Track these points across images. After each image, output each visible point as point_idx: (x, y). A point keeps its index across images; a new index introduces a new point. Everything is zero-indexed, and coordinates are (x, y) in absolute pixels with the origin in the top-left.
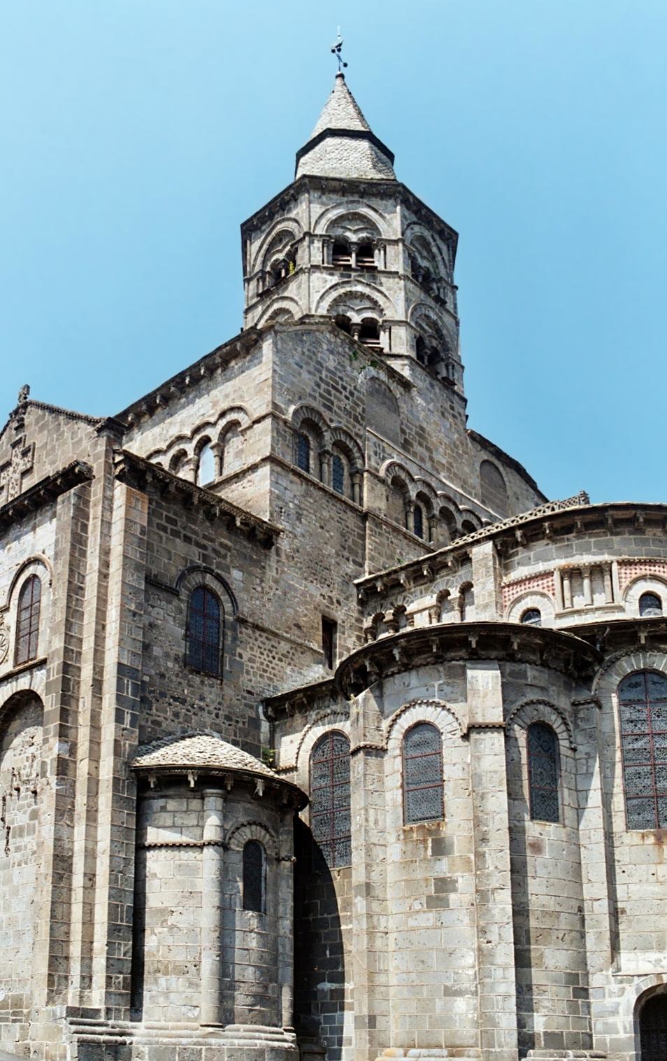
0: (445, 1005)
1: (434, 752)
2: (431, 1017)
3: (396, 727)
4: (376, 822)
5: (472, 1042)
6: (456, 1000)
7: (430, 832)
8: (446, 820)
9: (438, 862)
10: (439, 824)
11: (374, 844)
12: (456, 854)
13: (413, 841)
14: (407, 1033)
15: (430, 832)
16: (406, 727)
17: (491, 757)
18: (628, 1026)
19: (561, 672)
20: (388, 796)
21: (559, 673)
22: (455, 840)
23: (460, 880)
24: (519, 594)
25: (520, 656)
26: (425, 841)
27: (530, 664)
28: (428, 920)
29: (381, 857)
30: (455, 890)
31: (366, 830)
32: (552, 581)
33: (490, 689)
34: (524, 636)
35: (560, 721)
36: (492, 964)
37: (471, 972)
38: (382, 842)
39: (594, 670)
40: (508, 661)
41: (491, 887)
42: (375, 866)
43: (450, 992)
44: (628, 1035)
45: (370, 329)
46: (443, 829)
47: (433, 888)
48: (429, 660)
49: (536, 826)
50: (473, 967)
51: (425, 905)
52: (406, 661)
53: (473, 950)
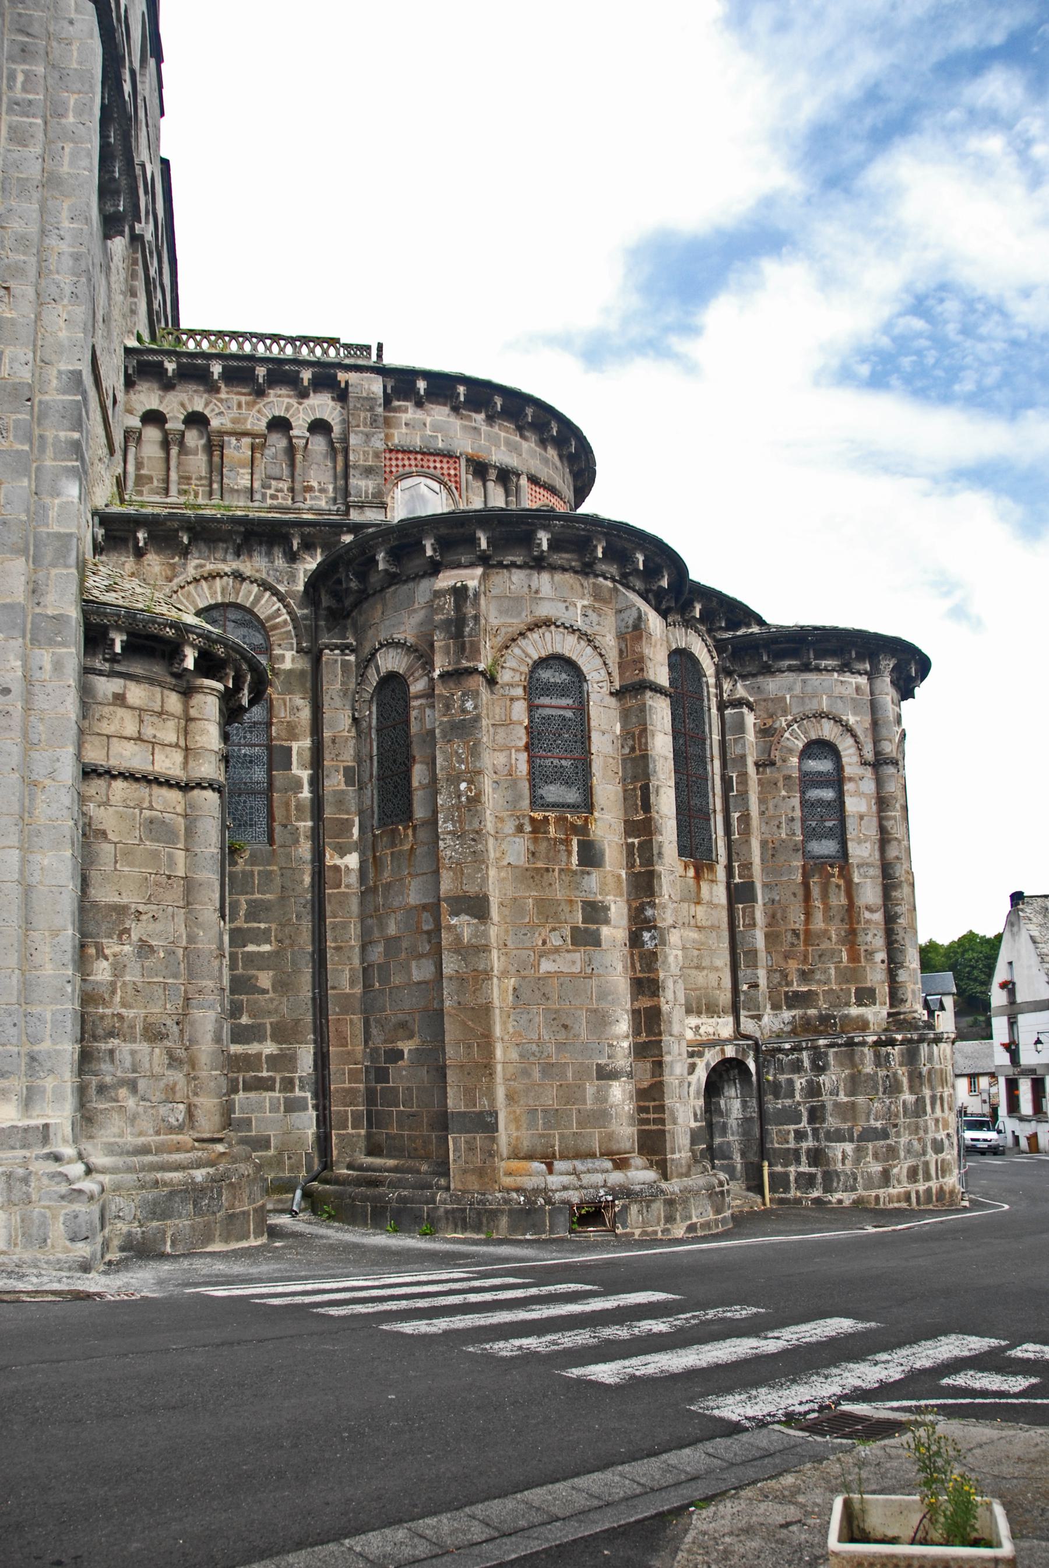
0: (598, 1092)
2: (579, 1111)
7: (575, 829)
8: (596, 814)
9: (586, 877)
10: (586, 818)
12: (608, 868)
13: (548, 839)
14: (542, 1136)
15: (575, 829)
16: (536, 657)
18: (699, 1112)
22: (606, 846)
24: (407, 469)
26: (567, 842)
28: (574, 963)
30: (607, 922)
32: (455, 469)
37: (625, 1044)
43: (606, 1074)
44: (698, 1124)
46: (592, 827)
50: (627, 1037)
53: (627, 1011)
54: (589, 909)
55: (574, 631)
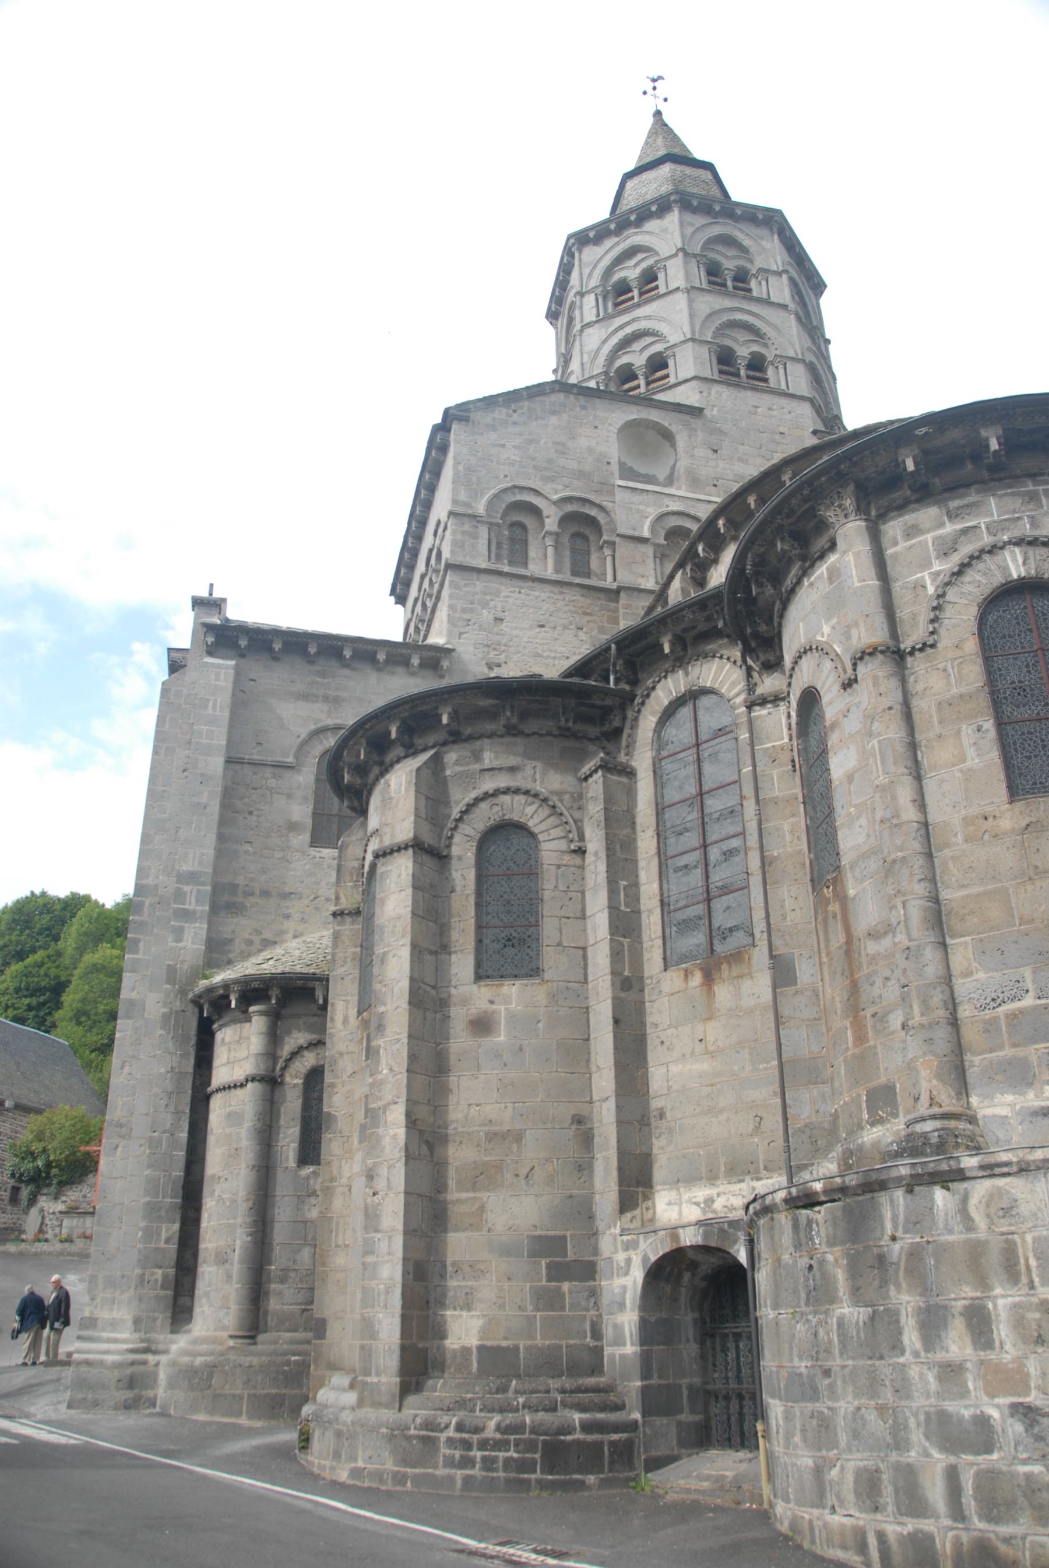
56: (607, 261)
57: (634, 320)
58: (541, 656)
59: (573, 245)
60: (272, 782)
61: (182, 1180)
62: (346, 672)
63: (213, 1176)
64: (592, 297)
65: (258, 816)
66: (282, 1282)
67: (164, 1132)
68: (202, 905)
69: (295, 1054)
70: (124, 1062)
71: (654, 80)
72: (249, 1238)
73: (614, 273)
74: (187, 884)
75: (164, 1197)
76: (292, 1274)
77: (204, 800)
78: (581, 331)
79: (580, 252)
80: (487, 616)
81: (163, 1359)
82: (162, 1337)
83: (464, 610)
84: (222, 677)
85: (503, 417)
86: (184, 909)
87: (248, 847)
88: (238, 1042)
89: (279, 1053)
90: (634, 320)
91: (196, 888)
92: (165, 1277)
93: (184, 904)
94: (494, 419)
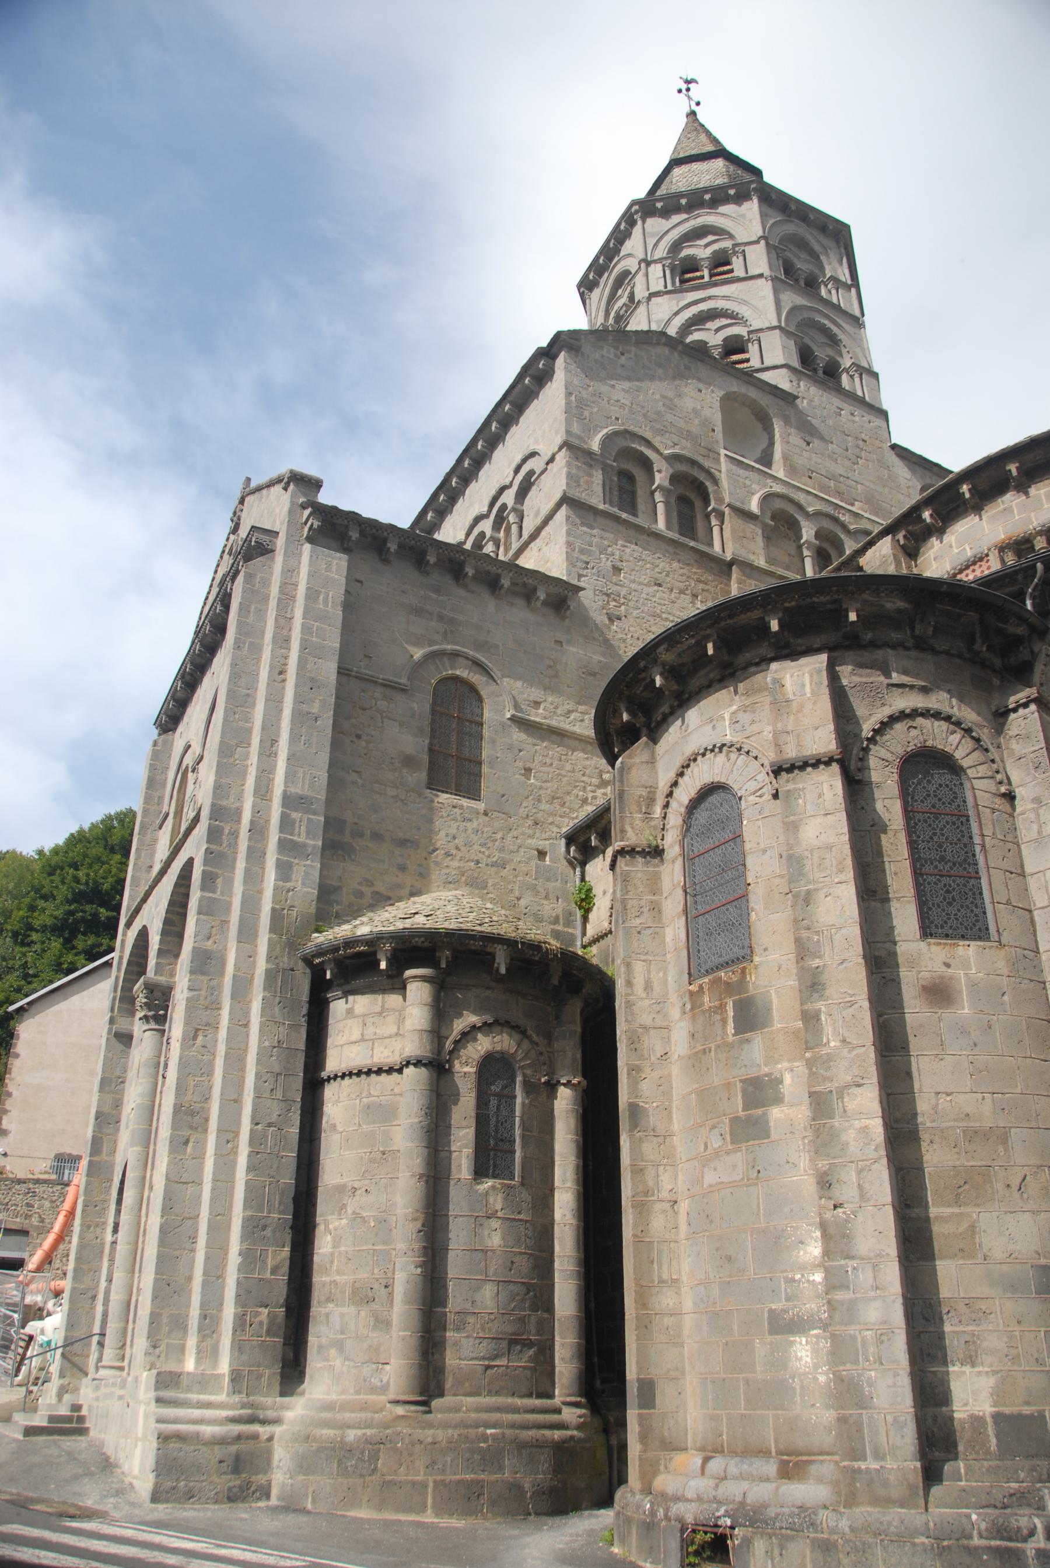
1: (731, 836)
3: (674, 804)
4: (648, 986)
5: (827, 1440)
6: (792, 1343)
7: (729, 988)
9: (745, 1046)
10: (743, 971)
11: (646, 1028)
13: (704, 1012)
15: (729, 988)
16: (686, 802)
17: (819, 820)
19: (960, 656)
20: (669, 934)
21: (957, 661)
23: (788, 1079)
25: (869, 636)
26: (722, 1007)
27: (893, 647)
28: (734, 1167)
29: (659, 1052)
30: (778, 1100)
31: (628, 1002)
33: (808, 695)
34: (867, 596)
35: (968, 744)
36: (849, 1257)
38: (659, 1022)
39: (1032, 652)
40: (848, 648)
41: (834, 1085)
42: (648, 1070)
45: (735, 346)
46: (752, 978)
47: (740, 1101)
48: (712, 675)
49: (934, 949)
51: (728, 1139)
52: (675, 687)
54: (751, 1089)
55: (721, 748)
56: (675, 234)
57: (710, 298)
58: (660, 617)
59: (636, 212)
60: (383, 704)
61: (293, 1189)
62: (462, 592)
63: (341, 1189)
64: (659, 267)
65: (367, 742)
66: (458, 1329)
67: (270, 1125)
68: (314, 839)
69: (468, 1035)
70: (197, 1030)
71: (688, 82)
72: (419, 1270)
73: (682, 249)
74: (296, 810)
75: (269, 1212)
76: (471, 1319)
77: (315, 710)
78: (649, 299)
79: (644, 222)
80: (606, 564)
81: (277, 1430)
82: (270, 1401)
83: (582, 551)
84: (334, 568)
85: (612, 356)
86: (292, 840)
87: (354, 777)
88: (380, 1013)
89: (444, 1032)
90: (710, 298)
91: (306, 816)
92: (272, 1317)
93: (291, 835)
94: (603, 356)
